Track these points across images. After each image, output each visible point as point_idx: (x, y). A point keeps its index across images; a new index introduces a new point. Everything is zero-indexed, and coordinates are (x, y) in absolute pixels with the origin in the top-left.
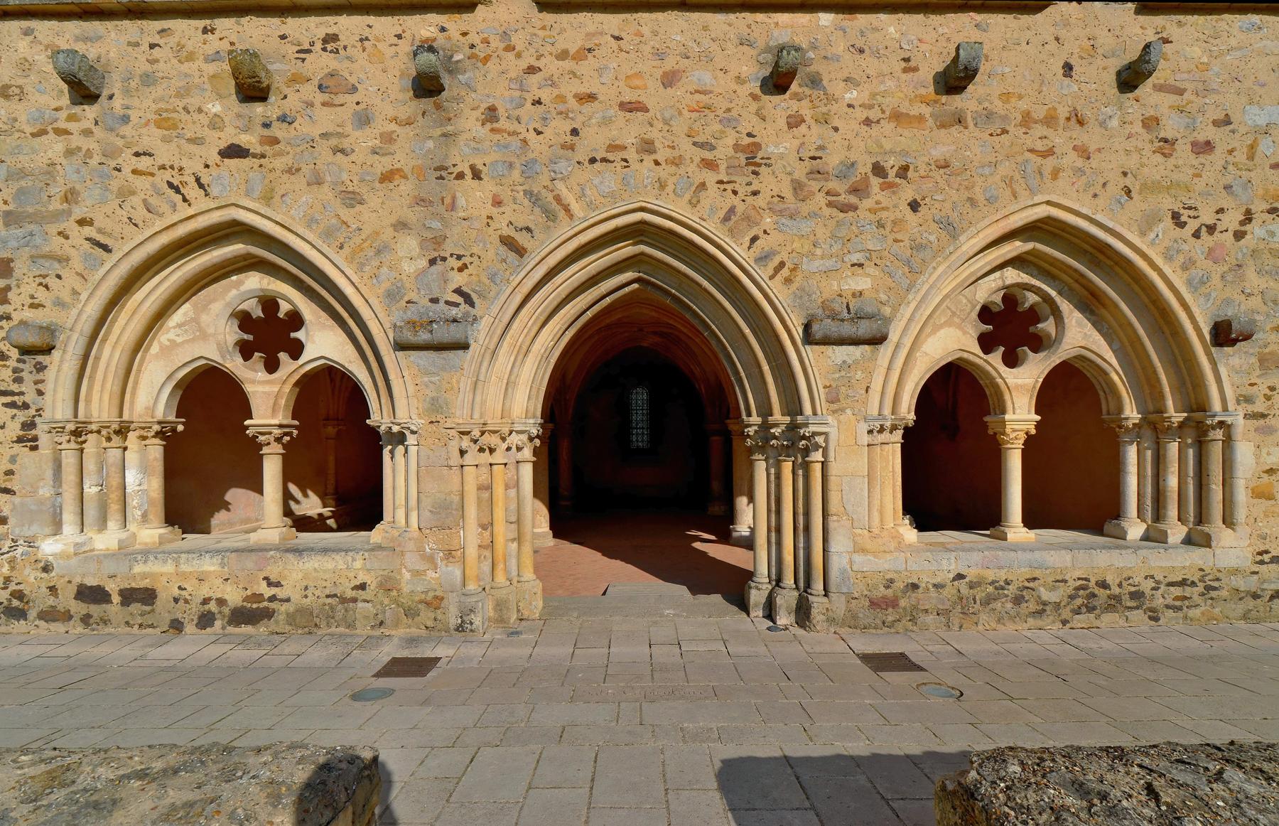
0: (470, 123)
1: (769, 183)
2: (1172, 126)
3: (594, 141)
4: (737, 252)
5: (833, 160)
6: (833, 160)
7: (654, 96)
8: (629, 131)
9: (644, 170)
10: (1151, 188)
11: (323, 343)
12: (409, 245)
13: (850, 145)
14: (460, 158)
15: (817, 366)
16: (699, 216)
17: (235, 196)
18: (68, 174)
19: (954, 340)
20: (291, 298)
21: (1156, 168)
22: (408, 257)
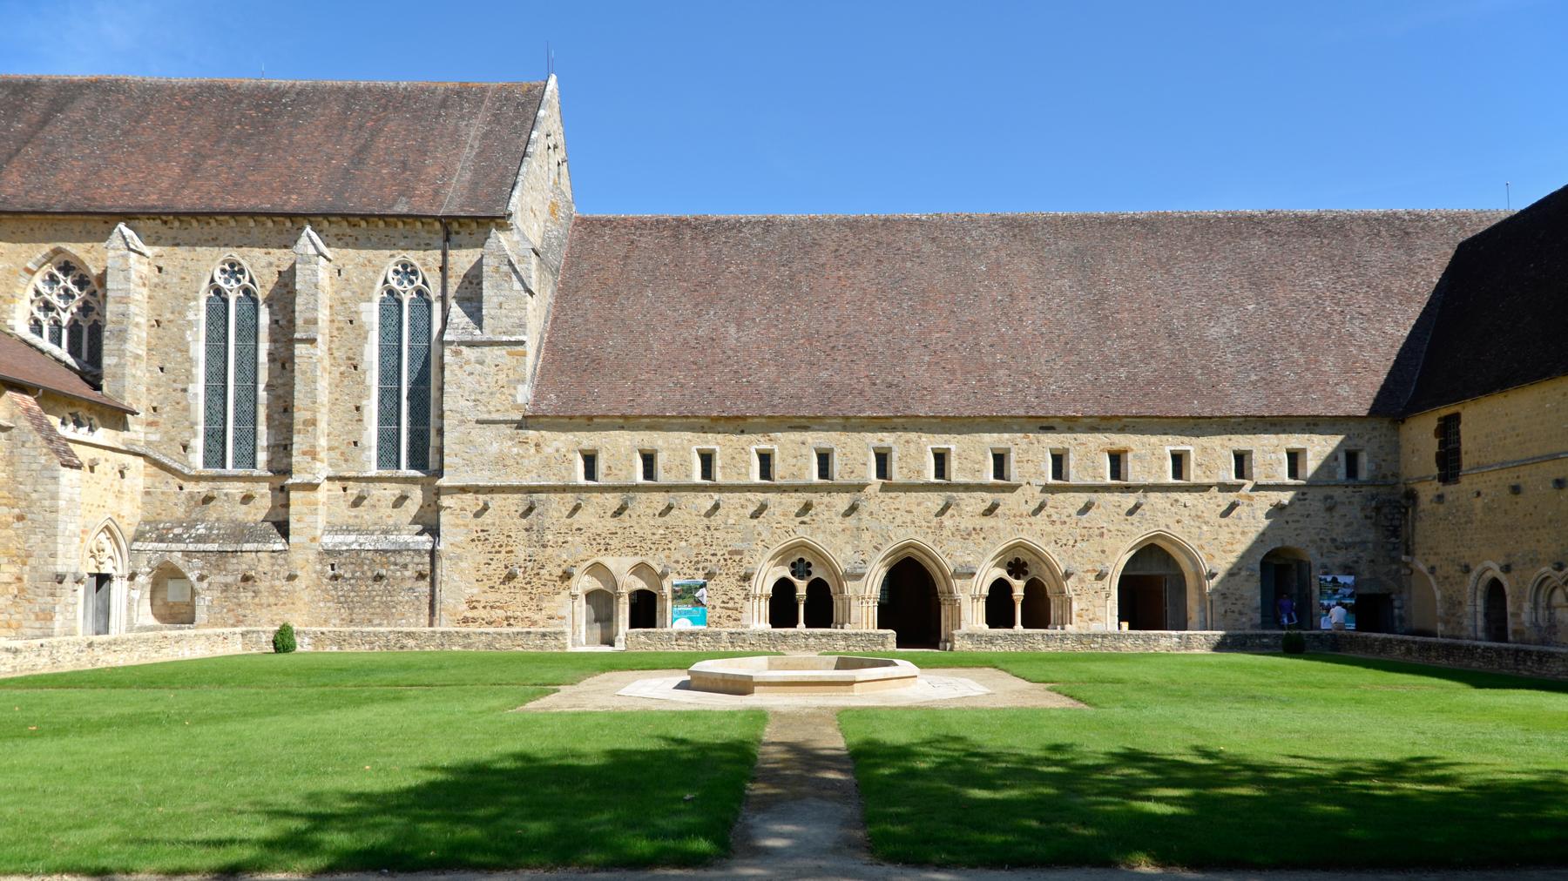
0: (865, 516)
1: (946, 533)
2: (1055, 517)
3: (899, 521)
4: (937, 551)
5: (962, 527)
6: (962, 527)
7: (914, 508)
8: (909, 518)
9: (912, 529)
10: (1049, 534)
11: (817, 573)
12: (849, 547)
13: (967, 523)
14: (863, 525)
15: (957, 584)
16: (926, 542)
17: (802, 534)
18: (760, 529)
19: (1002, 573)
20: (807, 559)
21: (1050, 528)
22: (849, 550)
